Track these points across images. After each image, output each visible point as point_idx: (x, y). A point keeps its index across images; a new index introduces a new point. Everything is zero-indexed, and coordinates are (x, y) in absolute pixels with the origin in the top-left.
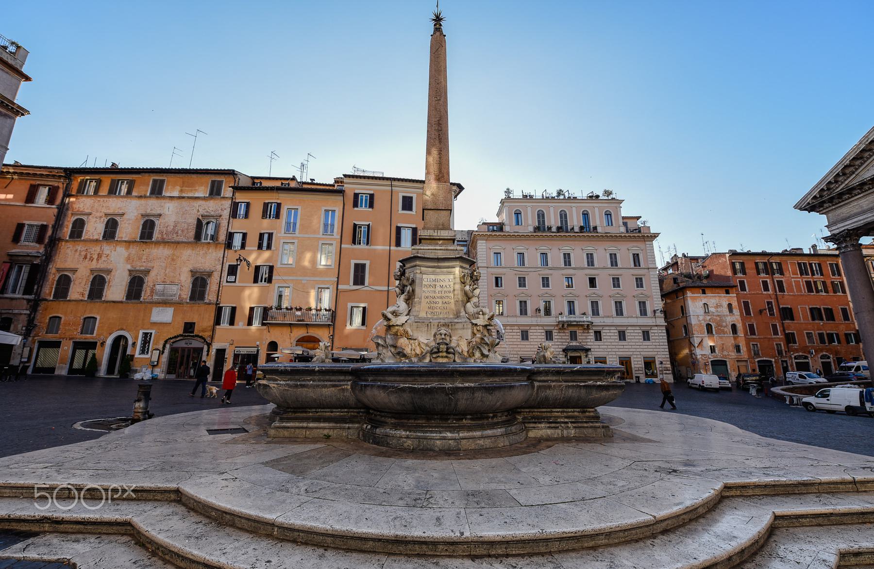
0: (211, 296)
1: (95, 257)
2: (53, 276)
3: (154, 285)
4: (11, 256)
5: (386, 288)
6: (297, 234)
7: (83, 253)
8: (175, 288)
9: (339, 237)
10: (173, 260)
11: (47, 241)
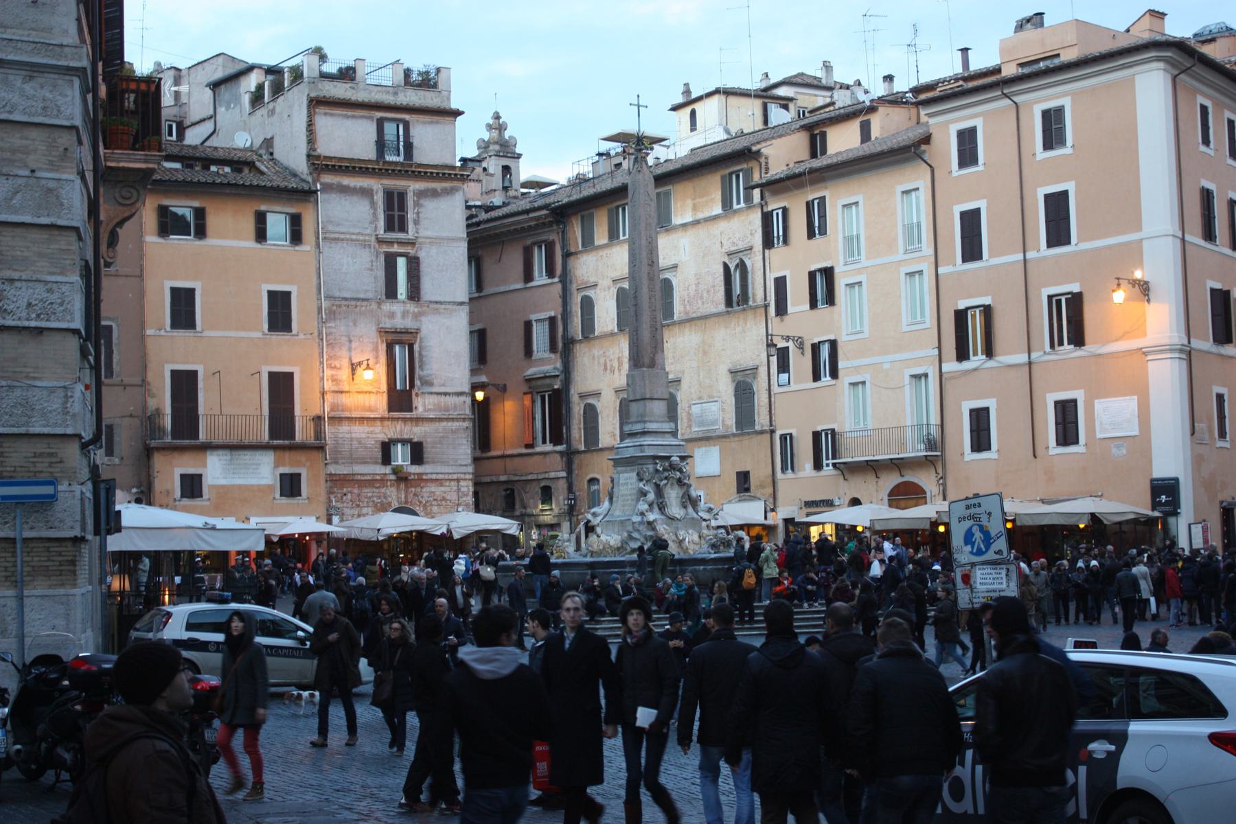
0: (761, 420)
1: (616, 364)
2: (577, 409)
3: (690, 407)
4: (529, 380)
5: (1022, 358)
6: (865, 262)
7: (602, 361)
8: (714, 407)
9: (931, 251)
10: (705, 353)
11: (560, 345)
